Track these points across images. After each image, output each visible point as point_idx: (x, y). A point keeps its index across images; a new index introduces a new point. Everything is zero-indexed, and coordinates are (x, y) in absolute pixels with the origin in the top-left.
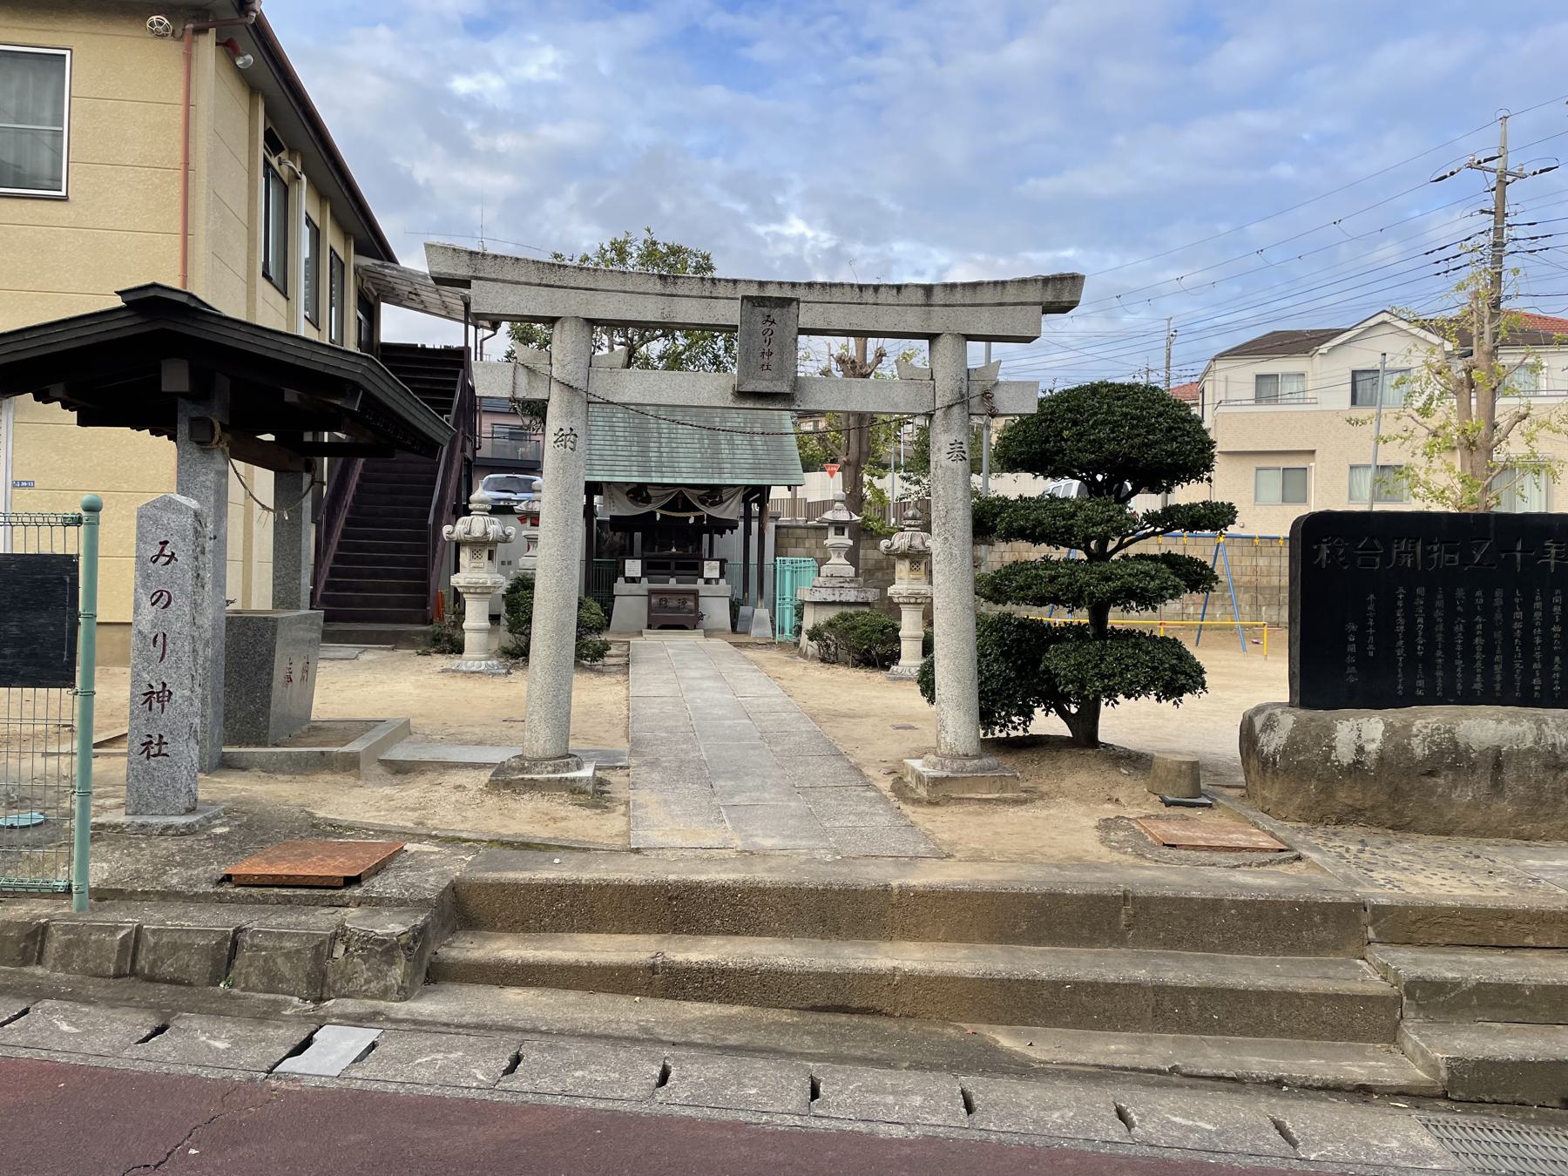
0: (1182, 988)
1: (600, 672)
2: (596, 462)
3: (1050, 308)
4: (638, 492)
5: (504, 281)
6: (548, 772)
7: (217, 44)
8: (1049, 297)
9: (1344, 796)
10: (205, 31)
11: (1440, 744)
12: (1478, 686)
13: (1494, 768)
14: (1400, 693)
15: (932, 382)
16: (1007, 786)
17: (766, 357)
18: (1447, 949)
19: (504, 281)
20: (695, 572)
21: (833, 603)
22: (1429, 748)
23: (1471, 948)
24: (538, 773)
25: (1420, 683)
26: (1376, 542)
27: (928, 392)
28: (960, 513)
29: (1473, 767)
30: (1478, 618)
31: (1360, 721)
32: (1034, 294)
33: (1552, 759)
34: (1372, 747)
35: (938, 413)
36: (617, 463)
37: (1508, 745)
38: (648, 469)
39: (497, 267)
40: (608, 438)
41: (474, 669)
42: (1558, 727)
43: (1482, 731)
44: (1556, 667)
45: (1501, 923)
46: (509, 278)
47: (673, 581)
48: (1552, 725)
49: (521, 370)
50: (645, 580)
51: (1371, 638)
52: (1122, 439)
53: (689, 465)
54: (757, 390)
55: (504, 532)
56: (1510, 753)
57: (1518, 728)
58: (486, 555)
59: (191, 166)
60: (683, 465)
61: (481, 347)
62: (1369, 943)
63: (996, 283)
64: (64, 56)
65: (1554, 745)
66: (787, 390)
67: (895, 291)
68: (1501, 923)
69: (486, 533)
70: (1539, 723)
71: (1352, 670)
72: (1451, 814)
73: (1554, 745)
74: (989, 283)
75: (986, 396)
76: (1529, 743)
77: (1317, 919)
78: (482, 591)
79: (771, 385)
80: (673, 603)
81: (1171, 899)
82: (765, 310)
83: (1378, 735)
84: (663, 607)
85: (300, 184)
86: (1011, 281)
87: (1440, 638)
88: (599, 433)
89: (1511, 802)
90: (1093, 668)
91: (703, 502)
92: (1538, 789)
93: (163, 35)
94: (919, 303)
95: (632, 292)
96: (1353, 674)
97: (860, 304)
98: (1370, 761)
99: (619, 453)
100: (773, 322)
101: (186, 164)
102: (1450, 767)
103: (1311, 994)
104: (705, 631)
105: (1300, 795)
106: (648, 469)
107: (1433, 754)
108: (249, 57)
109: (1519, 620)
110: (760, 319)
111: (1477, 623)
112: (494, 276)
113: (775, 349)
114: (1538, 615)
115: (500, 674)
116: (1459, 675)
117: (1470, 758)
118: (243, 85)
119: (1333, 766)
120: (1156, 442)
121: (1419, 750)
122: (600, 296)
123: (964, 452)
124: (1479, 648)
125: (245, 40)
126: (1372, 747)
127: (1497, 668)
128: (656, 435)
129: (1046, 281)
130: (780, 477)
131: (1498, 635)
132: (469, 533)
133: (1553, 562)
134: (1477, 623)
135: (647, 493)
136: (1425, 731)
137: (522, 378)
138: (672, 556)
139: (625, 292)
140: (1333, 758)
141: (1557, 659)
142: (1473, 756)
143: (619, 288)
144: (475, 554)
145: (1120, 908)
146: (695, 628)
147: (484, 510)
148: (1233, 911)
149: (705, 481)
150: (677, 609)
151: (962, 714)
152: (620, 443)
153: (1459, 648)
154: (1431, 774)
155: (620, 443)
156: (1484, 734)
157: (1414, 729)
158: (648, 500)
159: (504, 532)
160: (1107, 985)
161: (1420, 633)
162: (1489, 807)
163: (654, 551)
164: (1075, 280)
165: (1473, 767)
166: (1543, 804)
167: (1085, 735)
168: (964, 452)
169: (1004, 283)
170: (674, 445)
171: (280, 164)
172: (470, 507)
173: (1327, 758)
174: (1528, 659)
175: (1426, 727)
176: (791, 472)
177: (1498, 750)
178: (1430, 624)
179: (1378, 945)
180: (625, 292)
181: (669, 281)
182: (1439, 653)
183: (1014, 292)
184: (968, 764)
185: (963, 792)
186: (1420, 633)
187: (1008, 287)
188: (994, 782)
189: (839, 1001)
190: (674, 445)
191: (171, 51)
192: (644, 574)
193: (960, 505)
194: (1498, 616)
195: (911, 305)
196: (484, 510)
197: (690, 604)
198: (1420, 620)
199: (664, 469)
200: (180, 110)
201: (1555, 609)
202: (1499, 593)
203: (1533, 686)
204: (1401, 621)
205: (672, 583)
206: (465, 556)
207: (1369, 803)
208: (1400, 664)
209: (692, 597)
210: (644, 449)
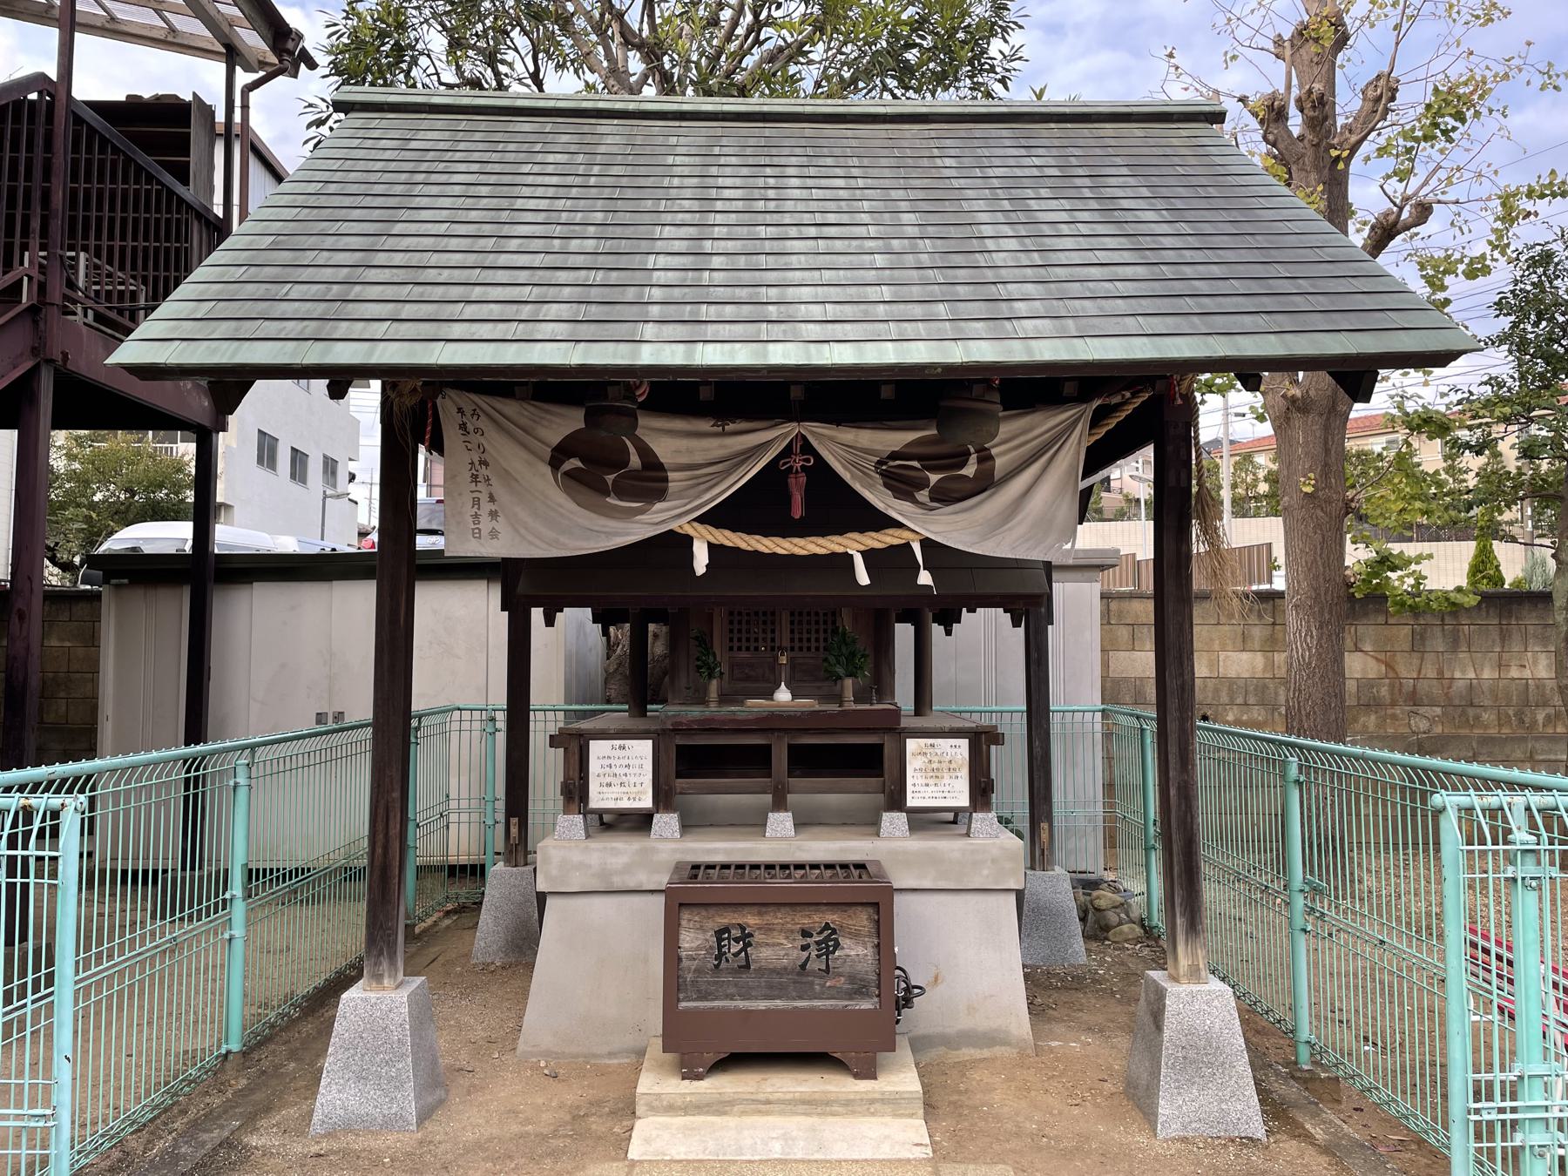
36: (477, 292)
47: (781, 823)
50: (666, 823)
53: (834, 293)
60: (806, 293)
61: (245, 107)
91: (902, 484)
135: (645, 452)
138: (777, 723)
163: (702, 701)
192: (663, 797)
197: (856, 952)
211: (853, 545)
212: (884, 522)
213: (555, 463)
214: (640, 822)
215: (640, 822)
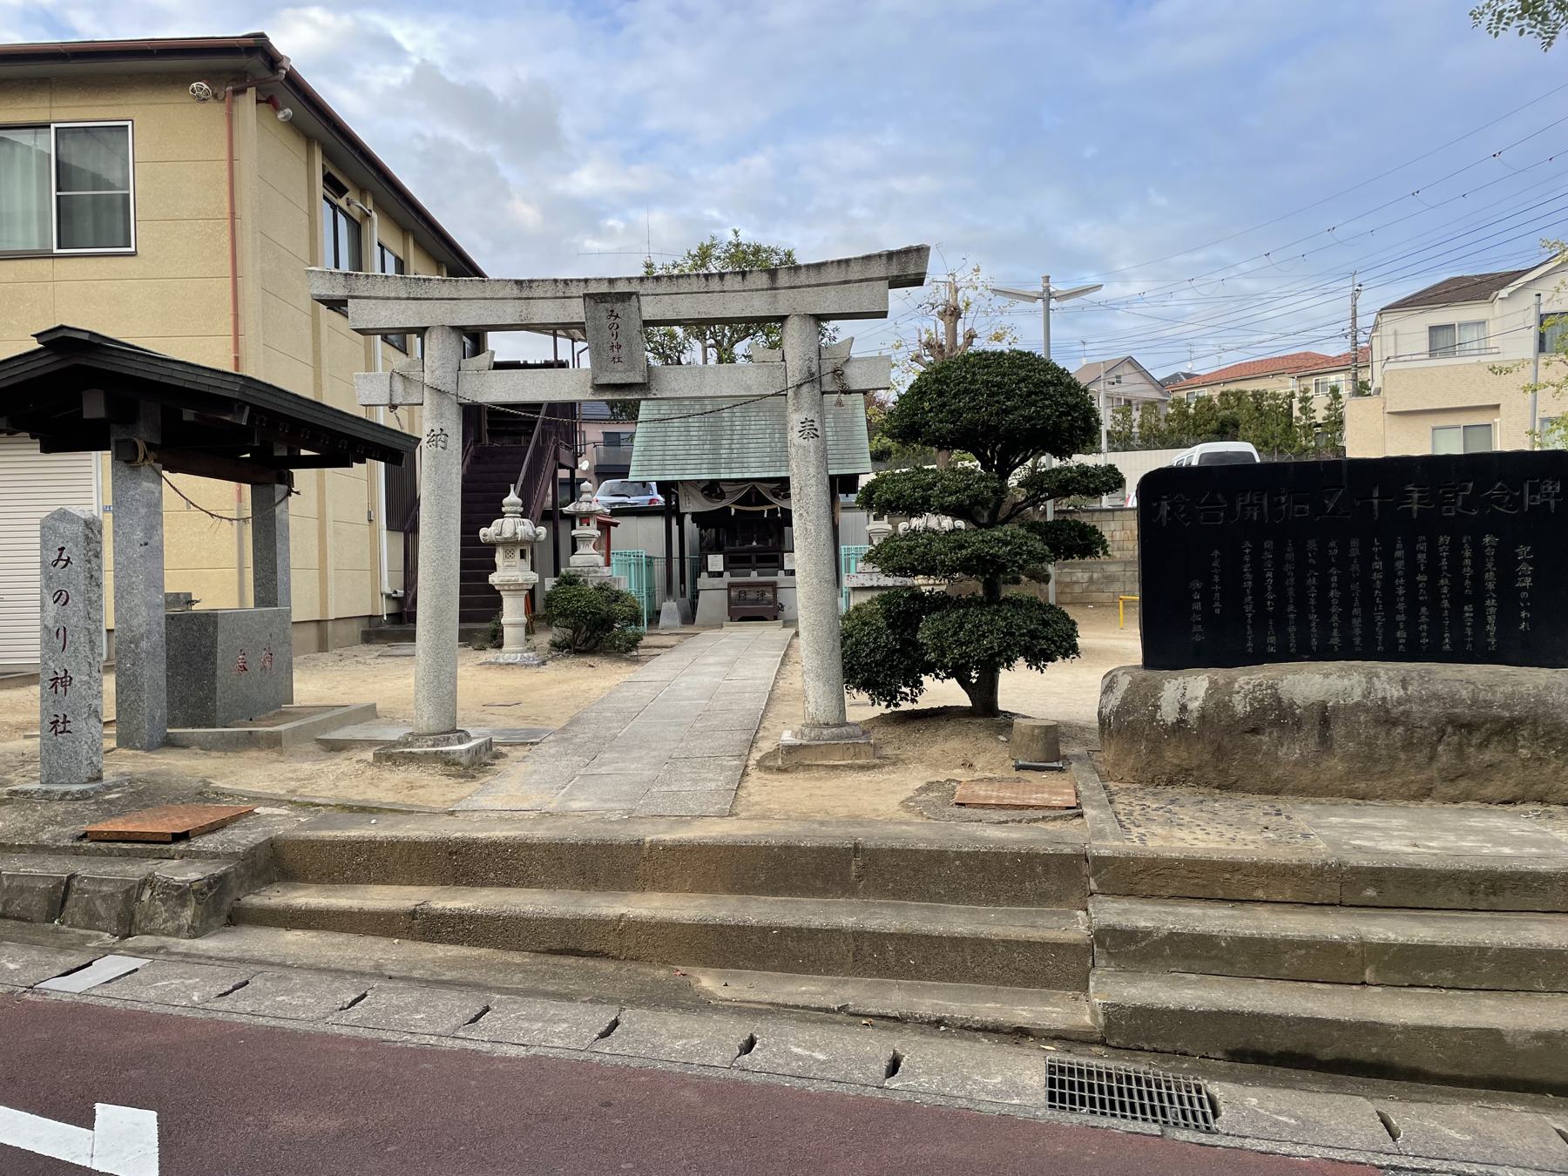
0: (880, 934)
1: (636, 661)
2: (669, 462)
3: (896, 283)
4: (712, 489)
5: (376, 298)
6: (428, 746)
7: (258, 102)
8: (894, 270)
9: (1173, 756)
10: (243, 91)
11: (1263, 700)
12: (1335, 641)
13: (1320, 724)
14: (1250, 650)
15: (783, 363)
16: (860, 752)
17: (615, 350)
18: (1171, 901)
19: (376, 298)
20: (776, 564)
21: (871, 588)
22: (1251, 705)
23: (1197, 901)
24: (419, 747)
25: (1272, 639)
26: (1219, 496)
27: (779, 373)
28: (814, 489)
29: (1298, 724)
30: (1333, 571)
31: (1187, 679)
32: (878, 270)
33: (1382, 713)
34: (1194, 706)
35: (790, 393)
36: (689, 462)
37: (1334, 700)
38: (718, 466)
39: (369, 285)
40: (682, 438)
41: (510, 661)
42: (1390, 679)
43: (1307, 686)
44: (1423, 619)
45: (1228, 876)
46: (381, 295)
47: (754, 574)
48: (1384, 677)
49: (397, 378)
50: (727, 574)
51: (1217, 595)
52: (982, 407)
54: (612, 382)
55: (535, 532)
56: (1336, 708)
57: (1346, 682)
58: (518, 553)
59: (238, 213)
60: (752, 460)
62: (1092, 894)
63: (839, 262)
64: (127, 126)
65: (1384, 699)
66: (639, 380)
67: (740, 278)
68: (1228, 876)
69: (516, 534)
70: (1370, 677)
71: (1199, 628)
72: (1278, 773)
73: (1384, 699)
74: (832, 262)
75: (838, 373)
76: (1357, 697)
77: (1039, 869)
78: (515, 588)
79: (624, 376)
80: (752, 595)
81: (898, 850)
82: (608, 306)
83: (1202, 694)
84: (741, 599)
85: (371, 221)
86: (855, 259)
87: (1291, 592)
88: (675, 434)
89: (1341, 759)
90: (952, 636)
91: (776, 495)
92: (1369, 745)
93: (204, 100)
94: (765, 287)
95: (493, 299)
96: (1200, 633)
97: (707, 292)
98: (1192, 718)
99: (692, 452)
100: (617, 316)
101: (233, 213)
102: (1273, 724)
103: (1003, 941)
104: (785, 622)
105: (1133, 756)
106: (718, 466)
107: (1254, 711)
108: (288, 111)
109: (1378, 571)
110: (604, 314)
111: (1332, 575)
112: (367, 294)
113: (622, 340)
114: (1400, 564)
115: (532, 665)
116: (1314, 630)
117: (1294, 714)
118: (298, 136)
119: (1158, 725)
120: (1016, 408)
121: (1240, 707)
122: (462, 304)
123: (816, 430)
124: (1335, 602)
125: (285, 94)
126: (1194, 706)
127: (1356, 622)
128: (729, 432)
129: (891, 255)
130: (847, 466)
131: (1355, 587)
132: (500, 534)
133: (1415, 507)
134: (1332, 575)
135: (721, 490)
136: (1246, 687)
137: (398, 385)
138: (753, 550)
139: (485, 299)
140: (1158, 717)
141: (1424, 609)
142: (1297, 711)
143: (480, 295)
144: (508, 555)
145: (851, 860)
146: (776, 618)
147: (515, 512)
148: (957, 863)
149: (772, 475)
150: (756, 601)
151: (821, 685)
152: (694, 443)
153: (1313, 602)
154: (1255, 731)
155: (694, 443)
156: (1309, 689)
157: (1236, 686)
158: (722, 496)
159: (535, 532)
160: (810, 930)
161: (1270, 588)
162: (1318, 765)
164: (920, 252)
165: (1298, 724)
166: (1376, 761)
167: (984, 706)
168: (816, 430)
169: (847, 261)
170: (745, 441)
171: (348, 205)
172: (503, 509)
173: (1153, 718)
174: (1390, 609)
175: (1248, 683)
176: (858, 461)
177: (1323, 706)
178: (1280, 577)
179: (1100, 897)
180: (485, 299)
181: (524, 285)
182: (1291, 608)
183: (859, 268)
184: (825, 732)
185: (816, 759)
186: (1270, 588)
187: (852, 264)
188: (848, 749)
189: (571, 944)
190: (745, 441)
191: (215, 112)
192: (726, 568)
193: (813, 481)
194: (1355, 567)
195: (757, 290)
196: (515, 512)
197: (769, 595)
198: (1270, 575)
199: (733, 465)
200: (225, 165)
201: (1419, 556)
202: (1355, 543)
203: (1398, 639)
204: (1248, 576)
205: (754, 576)
206: (499, 558)
207: (1195, 763)
208: (1250, 621)
209: (770, 589)
210: (715, 447)
211: (765, 508)
212: (772, 503)
213: (702, 491)
214: (720, 574)
215: (720, 574)
